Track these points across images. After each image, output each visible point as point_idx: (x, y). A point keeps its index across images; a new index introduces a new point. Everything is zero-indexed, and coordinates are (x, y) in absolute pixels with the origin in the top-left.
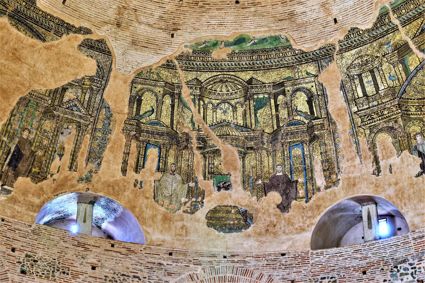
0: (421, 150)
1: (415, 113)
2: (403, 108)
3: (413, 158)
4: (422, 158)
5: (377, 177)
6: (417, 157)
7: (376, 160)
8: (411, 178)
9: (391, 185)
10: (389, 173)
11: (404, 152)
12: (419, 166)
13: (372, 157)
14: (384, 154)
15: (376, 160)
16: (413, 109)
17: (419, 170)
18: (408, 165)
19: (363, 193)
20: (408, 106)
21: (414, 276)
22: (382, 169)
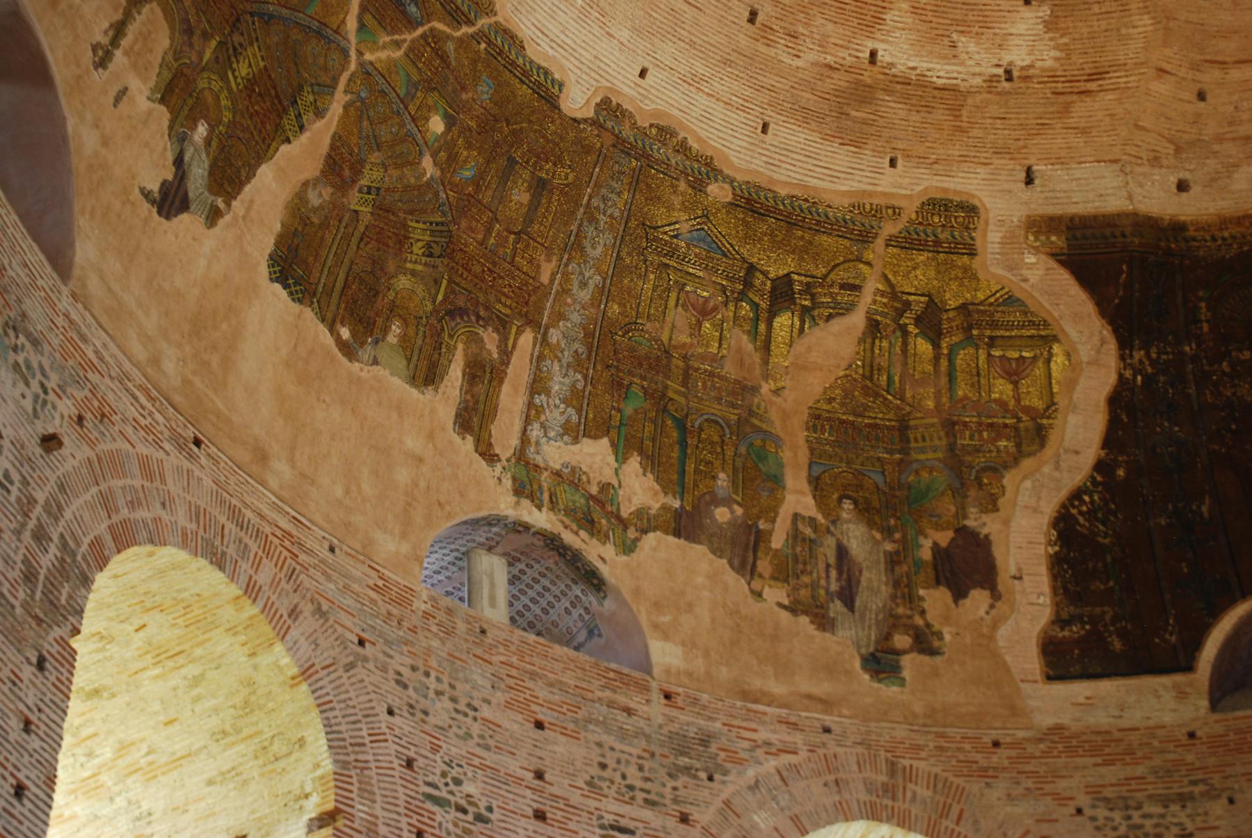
0: (187, 158)
1: (239, 80)
2: (237, 38)
3: (165, 149)
4: (176, 175)
5: (92, 68)
6: (170, 157)
7: (119, 30)
8: (133, 178)
9: (97, 127)
10: (112, 101)
11: (163, 108)
12: (161, 180)
13: (119, 16)
14: (136, 48)
15: (119, 30)
16: (243, 70)
17: (154, 187)
18: (147, 145)
19: (52, 50)
20: (246, 50)
21: (38, 408)
22: (111, 66)
